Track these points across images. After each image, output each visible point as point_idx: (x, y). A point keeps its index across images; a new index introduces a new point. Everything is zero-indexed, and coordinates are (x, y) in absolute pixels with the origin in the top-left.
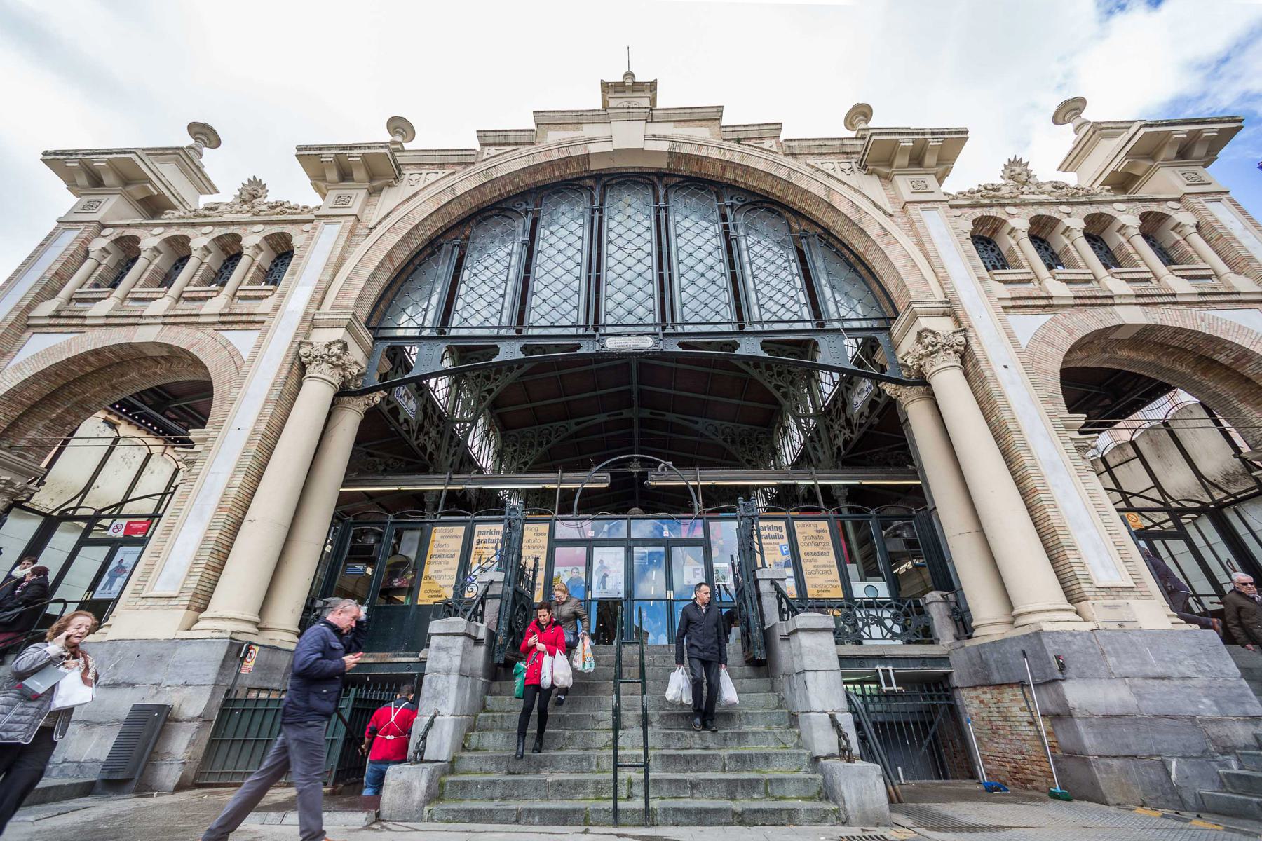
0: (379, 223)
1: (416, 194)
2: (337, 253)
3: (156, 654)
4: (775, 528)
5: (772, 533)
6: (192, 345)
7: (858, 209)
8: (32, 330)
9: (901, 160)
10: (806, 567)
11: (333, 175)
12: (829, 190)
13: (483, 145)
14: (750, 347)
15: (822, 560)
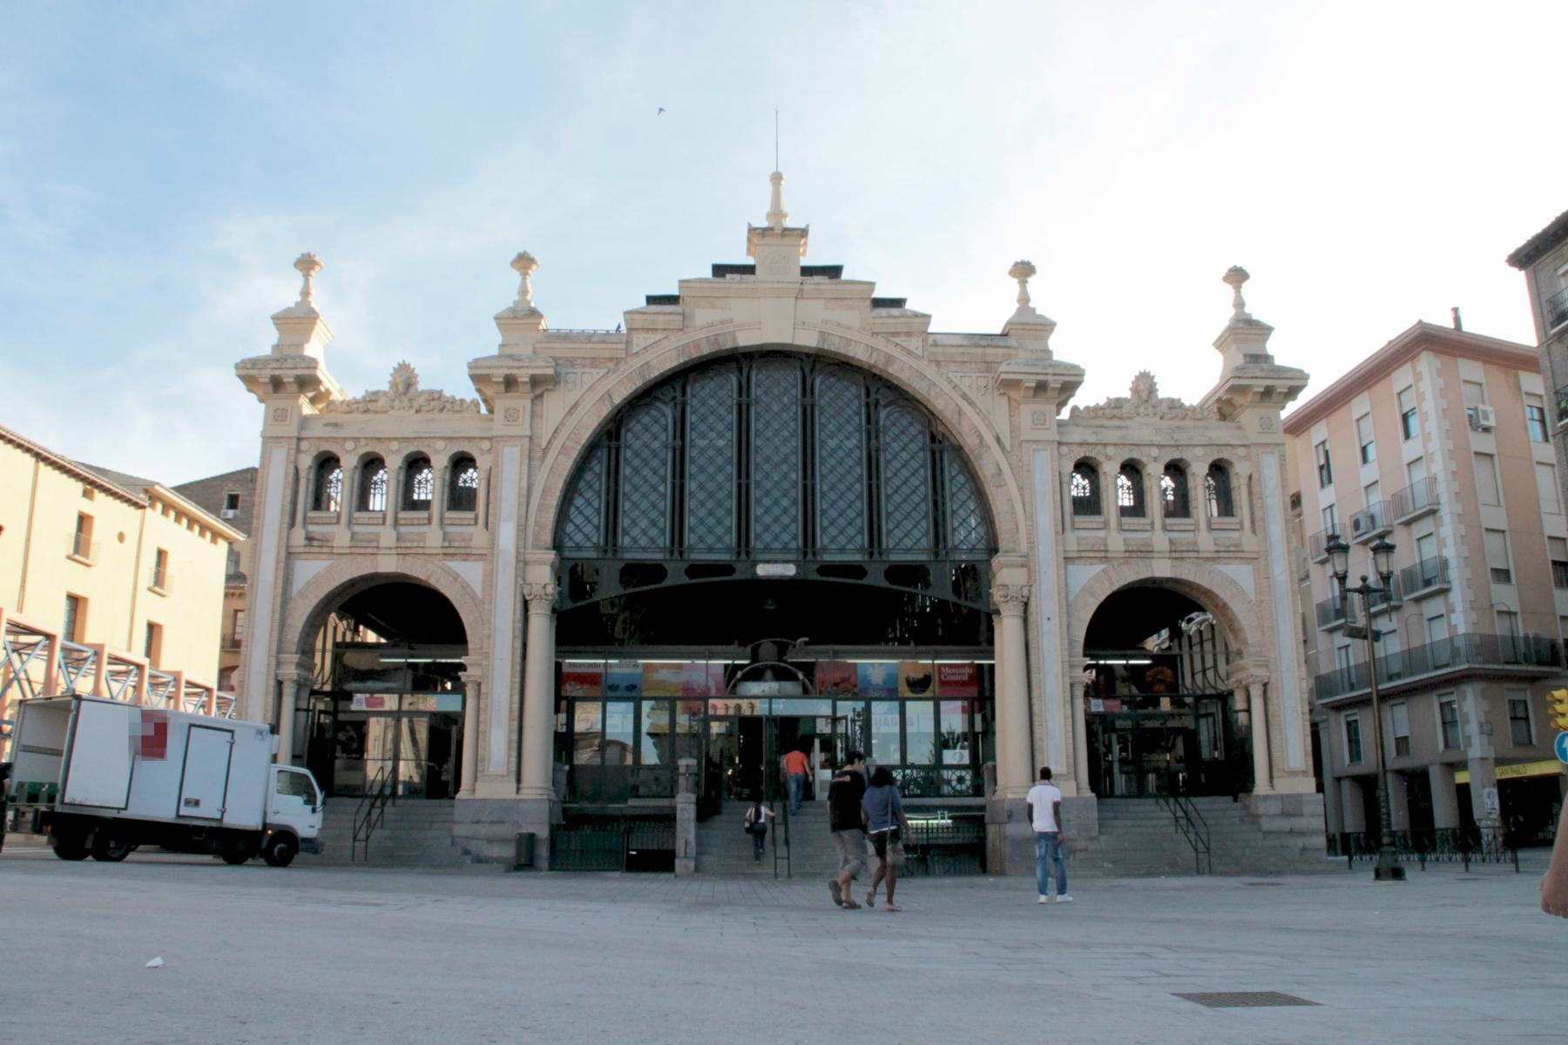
1: (576, 406)
2: (525, 484)
3: (505, 806)
12: (960, 412)
14: (876, 578)
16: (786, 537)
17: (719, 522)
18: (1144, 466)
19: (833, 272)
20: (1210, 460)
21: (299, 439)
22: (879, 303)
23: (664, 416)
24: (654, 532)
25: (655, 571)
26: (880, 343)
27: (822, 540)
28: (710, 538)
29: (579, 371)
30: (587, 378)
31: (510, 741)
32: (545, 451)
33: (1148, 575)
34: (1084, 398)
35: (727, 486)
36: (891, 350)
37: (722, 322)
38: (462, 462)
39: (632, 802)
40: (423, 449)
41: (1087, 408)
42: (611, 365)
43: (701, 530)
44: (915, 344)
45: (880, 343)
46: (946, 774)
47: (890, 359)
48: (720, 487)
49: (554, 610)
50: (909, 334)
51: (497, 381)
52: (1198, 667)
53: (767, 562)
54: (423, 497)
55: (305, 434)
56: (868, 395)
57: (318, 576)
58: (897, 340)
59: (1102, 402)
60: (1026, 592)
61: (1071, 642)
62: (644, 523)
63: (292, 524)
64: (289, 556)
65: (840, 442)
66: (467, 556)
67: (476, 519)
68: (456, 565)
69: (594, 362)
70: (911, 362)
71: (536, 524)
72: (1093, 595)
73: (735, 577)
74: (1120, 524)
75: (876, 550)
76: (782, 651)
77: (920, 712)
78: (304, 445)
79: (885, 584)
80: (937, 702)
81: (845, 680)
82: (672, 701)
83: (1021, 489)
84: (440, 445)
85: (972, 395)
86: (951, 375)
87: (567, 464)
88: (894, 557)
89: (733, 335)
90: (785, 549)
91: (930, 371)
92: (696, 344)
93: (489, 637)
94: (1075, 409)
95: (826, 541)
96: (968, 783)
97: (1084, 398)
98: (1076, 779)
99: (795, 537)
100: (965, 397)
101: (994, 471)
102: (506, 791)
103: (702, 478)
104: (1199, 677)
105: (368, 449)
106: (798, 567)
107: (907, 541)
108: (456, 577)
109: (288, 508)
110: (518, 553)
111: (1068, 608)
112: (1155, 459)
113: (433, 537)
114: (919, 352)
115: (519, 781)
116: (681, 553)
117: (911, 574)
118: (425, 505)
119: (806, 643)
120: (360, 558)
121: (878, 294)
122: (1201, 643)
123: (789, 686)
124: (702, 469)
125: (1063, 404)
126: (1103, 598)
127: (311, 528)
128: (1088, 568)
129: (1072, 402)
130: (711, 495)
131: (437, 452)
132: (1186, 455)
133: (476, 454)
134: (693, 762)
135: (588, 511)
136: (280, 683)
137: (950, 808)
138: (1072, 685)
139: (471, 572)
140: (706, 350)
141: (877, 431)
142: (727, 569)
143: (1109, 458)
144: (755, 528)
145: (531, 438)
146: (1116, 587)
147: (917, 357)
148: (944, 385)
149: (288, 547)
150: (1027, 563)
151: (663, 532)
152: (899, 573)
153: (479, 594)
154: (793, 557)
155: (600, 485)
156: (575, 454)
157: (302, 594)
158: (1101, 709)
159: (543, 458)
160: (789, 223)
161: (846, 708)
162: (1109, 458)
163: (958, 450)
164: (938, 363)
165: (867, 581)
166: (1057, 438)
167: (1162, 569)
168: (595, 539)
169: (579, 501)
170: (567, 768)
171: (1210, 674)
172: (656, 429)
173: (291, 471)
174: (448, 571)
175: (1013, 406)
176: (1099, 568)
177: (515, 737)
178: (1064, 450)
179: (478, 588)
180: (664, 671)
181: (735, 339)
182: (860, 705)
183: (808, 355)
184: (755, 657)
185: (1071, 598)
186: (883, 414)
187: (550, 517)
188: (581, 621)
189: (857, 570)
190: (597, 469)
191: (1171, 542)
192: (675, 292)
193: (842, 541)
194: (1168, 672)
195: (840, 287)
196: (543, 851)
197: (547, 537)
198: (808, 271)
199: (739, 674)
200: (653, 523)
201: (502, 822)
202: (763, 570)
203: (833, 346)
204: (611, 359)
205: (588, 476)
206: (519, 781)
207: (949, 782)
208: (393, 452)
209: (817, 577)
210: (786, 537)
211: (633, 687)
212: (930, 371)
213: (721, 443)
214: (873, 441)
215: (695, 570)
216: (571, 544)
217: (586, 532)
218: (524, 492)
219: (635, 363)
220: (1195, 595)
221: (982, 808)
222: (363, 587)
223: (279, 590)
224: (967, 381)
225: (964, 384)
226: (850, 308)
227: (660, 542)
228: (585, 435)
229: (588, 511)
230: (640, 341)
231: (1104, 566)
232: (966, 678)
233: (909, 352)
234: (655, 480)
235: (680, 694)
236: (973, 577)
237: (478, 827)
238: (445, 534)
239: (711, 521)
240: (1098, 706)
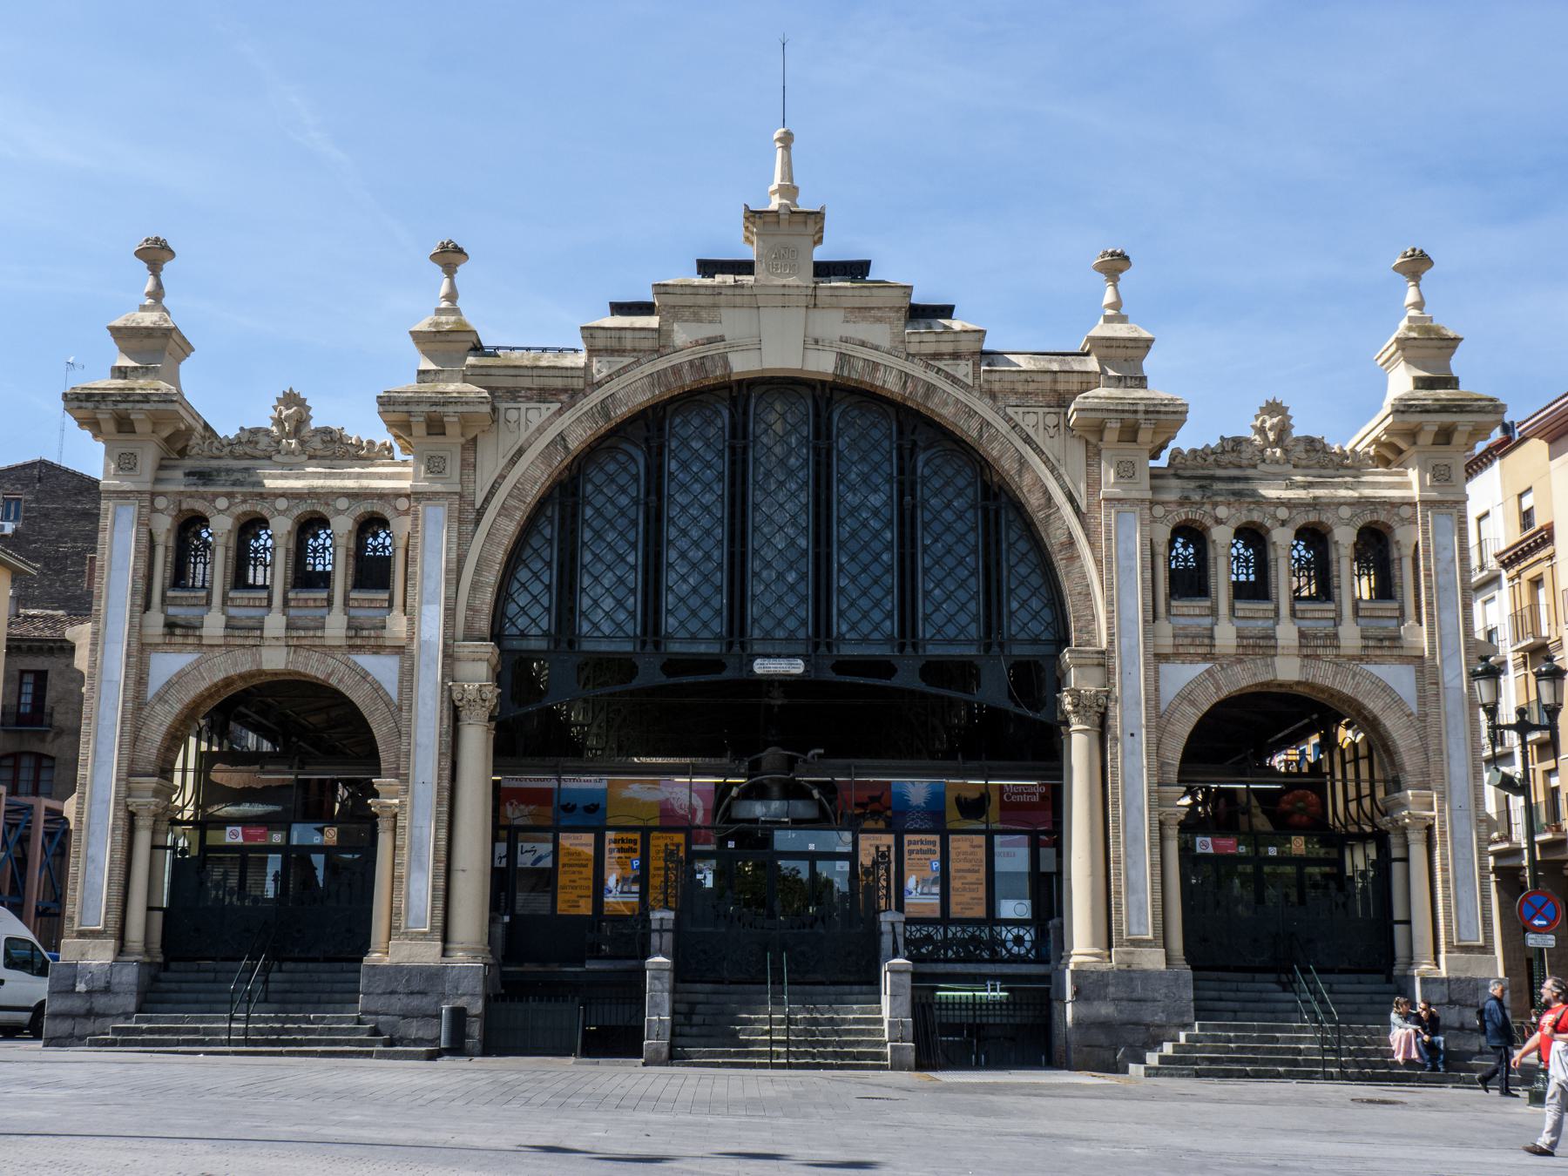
0: (487, 500)
2: (454, 555)
4: (928, 842)
5: (925, 847)
6: (330, 675)
7: (1049, 499)
8: (148, 649)
9: (1111, 436)
10: (955, 884)
11: (419, 430)
12: (1023, 462)
13: (592, 352)
14: (907, 678)
15: (971, 877)
16: (791, 623)
17: (706, 602)
18: (1268, 531)
19: (857, 270)
20: (1360, 524)
21: (154, 495)
22: (922, 314)
23: (634, 460)
24: (621, 616)
25: (622, 667)
26: (917, 370)
27: (840, 627)
28: (692, 625)
29: (523, 406)
30: (533, 415)
31: (434, 888)
32: (480, 513)
33: (1269, 677)
34: (1187, 440)
35: (716, 554)
36: (931, 377)
37: (710, 341)
38: (371, 524)
39: (591, 965)
40: (321, 509)
41: (1194, 451)
42: (564, 397)
43: (683, 613)
44: (963, 370)
45: (917, 370)
46: (1008, 934)
47: (930, 389)
48: (708, 557)
49: (491, 718)
50: (956, 356)
51: (414, 419)
52: (1352, 793)
53: (768, 656)
54: (319, 568)
55: (161, 488)
56: (901, 433)
57: (181, 675)
58: (941, 364)
59: (1214, 442)
60: (1102, 701)
61: (1162, 765)
62: (608, 604)
63: (147, 607)
64: (140, 652)
65: (866, 500)
66: (378, 649)
67: (391, 601)
68: (365, 661)
69: (543, 395)
70: (960, 395)
71: (469, 607)
72: (1193, 703)
73: (727, 675)
74: (1232, 610)
75: (908, 640)
76: (791, 764)
77: (967, 849)
78: (161, 503)
79: (919, 685)
80: (990, 835)
81: (873, 799)
82: (646, 831)
83: (1098, 562)
84: (342, 503)
85: (1039, 440)
86: (1009, 410)
87: (510, 528)
88: (933, 651)
89: (724, 357)
90: (791, 638)
91: (983, 407)
92: (676, 370)
93: (408, 754)
94: (1176, 454)
95: (844, 628)
96: (1028, 945)
97: (1187, 440)
98: (1165, 946)
99: (804, 623)
100: (1028, 440)
101: (1064, 539)
102: (428, 954)
103: (683, 543)
104: (1353, 806)
105: (246, 507)
106: (807, 662)
107: (951, 623)
108: (365, 676)
109: (141, 585)
110: (445, 645)
111: (1159, 721)
112: (1283, 523)
113: (336, 625)
114: (970, 381)
115: (445, 939)
116: (657, 645)
117: (960, 673)
118: (324, 580)
119: (820, 756)
120: (238, 652)
121: (917, 298)
122: (1356, 760)
123: (802, 809)
124: (684, 533)
125: (1163, 447)
126: (1206, 708)
127: (171, 610)
128: (1187, 666)
129: (1172, 445)
130: (694, 566)
131: (339, 512)
132: (1327, 517)
133: (388, 514)
134: (670, 915)
135: (536, 588)
136: (132, 817)
137: (1004, 978)
138: (1161, 824)
139: (383, 669)
140: (689, 380)
141: (913, 484)
142: (715, 664)
143: (1219, 521)
144: (753, 610)
145: (461, 496)
146: (1224, 693)
147: (965, 387)
148: (1003, 427)
149: (140, 639)
150: (1103, 661)
151: (633, 615)
152: (935, 670)
153: (394, 694)
154: (801, 649)
155: (552, 553)
156: (519, 516)
157: (161, 697)
158: (1210, 850)
159: (477, 523)
160: (804, 204)
161: (869, 846)
162: (1219, 521)
163: (1019, 507)
164: (993, 396)
165: (895, 682)
166: (1148, 495)
167: (1288, 670)
168: (544, 624)
169: (523, 574)
170: (507, 919)
171: (1366, 803)
172: (623, 479)
173: (145, 538)
175: (1093, 454)
176: (1202, 667)
177: (441, 883)
178: (1159, 511)
179: (392, 690)
180: (636, 786)
181: (726, 364)
182: (888, 840)
183: (823, 383)
184: (754, 769)
185: (1163, 707)
186: (921, 458)
187: (487, 597)
188: (528, 729)
189: (883, 668)
190: (547, 532)
191: (1302, 635)
192: (648, 296)
193: (864, 627)
194: (1313, 797)
195: (866, 292)
196: (475, 1029)
197: (484, 624)
198: (824, 270)
199: (734, 792)
200: (620, 603)
201: (423, 993)
202: (761, 667)
203: (857, 373)
204: (565, 390)
205: (536, 542)
206: (445, 939)
207: (1003, 943)
208: (281, 513)
209: (831, 676)
210: (791, 623)
211: (592, 809)
212: (983, 407)
213: (708, 498)
214: (908, 498)
215: (674, 665)
216: (514, 631)
217: (533, 619)
218: (453, 566)
219: (596, 397)
220: (1334, 704)
221: (1046, 978)
222: (240, 686)
223: (131, 693)
224: (1031, 419)
225: (1028, 422)
226: (879, 320)
227: (629, 628)
228: (533, 493)
229: (536, 588)
230: (600, 369)
231: (1208, 666)
232: (1036, 799)
233: (955, 380)
234: (622, 547)
235: (655, 822)
236: (1037, 680)
237: (394, 999)
238: (350, 619)
239: (694, 602)
240: (1204, 845)
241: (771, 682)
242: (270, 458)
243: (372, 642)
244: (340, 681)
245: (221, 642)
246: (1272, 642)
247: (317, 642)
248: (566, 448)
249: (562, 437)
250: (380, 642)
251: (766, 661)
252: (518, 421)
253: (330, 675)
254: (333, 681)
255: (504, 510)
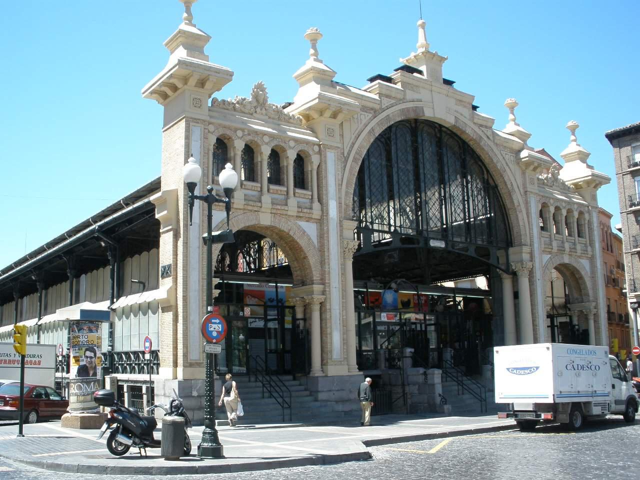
6: (290, 230)
14: (472, 252)
26: (476, 129)
36: (480, 133)
45: (476, 129)
58: (483, 129)
66: (309, 220)
68: (303, 224)
131: (290, 148)
148: (501, 158)
165: (469, 253)
174: (299, 227)
201: (343, 390)
219: (384, 114)
230: (386, 102)
237: (331, 393)
241: (435, 249)
242: (252, 114)
243: (307, 215)
244: (295, 233)
245: (242, 207)
246: (563, 249)
247: (285, 212)
248: (374, 135)
249: (373, 129)
250: (310, 216)
251: (435, 241)
252: (357, 118)
253: (290, 230)
254: (291, 233)
255: (355, 160)
